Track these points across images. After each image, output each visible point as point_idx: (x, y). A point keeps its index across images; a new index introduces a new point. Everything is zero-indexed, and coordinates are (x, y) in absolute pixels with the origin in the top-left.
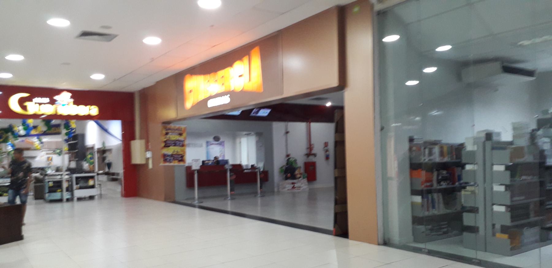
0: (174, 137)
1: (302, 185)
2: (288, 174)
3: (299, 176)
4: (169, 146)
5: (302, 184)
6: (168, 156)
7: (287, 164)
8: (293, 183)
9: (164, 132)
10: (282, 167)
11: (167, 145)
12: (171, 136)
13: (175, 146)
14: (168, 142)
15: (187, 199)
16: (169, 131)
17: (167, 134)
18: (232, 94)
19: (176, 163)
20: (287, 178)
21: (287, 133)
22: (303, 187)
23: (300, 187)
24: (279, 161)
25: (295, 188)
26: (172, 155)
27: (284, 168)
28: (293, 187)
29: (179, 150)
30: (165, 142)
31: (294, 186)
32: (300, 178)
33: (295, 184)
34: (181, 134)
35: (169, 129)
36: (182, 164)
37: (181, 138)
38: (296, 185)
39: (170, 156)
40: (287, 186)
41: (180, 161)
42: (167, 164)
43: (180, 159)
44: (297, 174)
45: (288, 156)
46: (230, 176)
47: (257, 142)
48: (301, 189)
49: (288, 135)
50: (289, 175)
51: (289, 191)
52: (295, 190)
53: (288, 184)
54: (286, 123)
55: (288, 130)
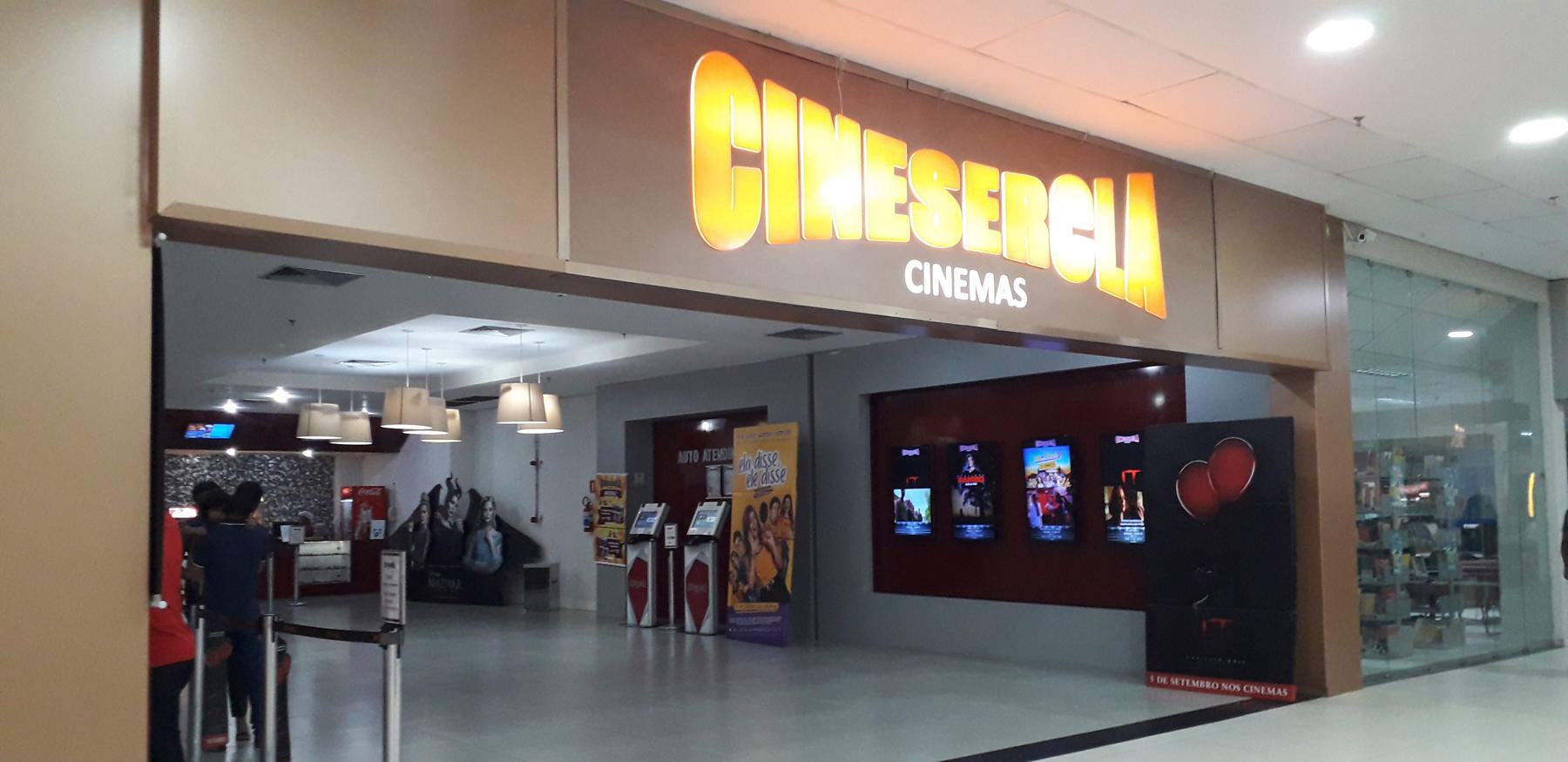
18: (1040, 279)
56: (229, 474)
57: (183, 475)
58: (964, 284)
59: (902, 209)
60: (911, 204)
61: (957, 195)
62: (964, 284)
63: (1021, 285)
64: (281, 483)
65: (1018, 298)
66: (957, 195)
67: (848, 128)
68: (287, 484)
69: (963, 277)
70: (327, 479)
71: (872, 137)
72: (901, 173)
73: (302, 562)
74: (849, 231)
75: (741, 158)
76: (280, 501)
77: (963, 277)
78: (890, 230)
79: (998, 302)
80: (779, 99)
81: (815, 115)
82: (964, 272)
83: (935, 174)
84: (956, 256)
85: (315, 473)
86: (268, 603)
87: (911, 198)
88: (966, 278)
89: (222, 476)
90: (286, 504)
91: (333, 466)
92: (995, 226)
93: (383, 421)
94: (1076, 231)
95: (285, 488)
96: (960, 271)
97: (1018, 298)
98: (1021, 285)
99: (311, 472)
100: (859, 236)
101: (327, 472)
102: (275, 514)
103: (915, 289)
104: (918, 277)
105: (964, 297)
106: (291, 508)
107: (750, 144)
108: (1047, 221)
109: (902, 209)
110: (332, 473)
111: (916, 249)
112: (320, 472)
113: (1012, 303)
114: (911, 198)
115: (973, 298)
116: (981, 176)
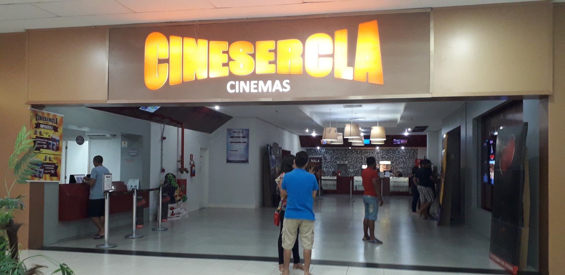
0: (47, 132)
1: (181, 211)
3: (178, 198)
7: (165, 182)
9: (34, 121)
12: (42, 130)
13: (48, 148)
15: (59, 241)
16: (41, 122)
17: (38, 126)
19: (47, 179)
21: (165, 138)
22: (182, 213)
23: (179, 213)
24: (155, 180)
25: (174, 215)
29: (52, 157)
32: (180, 200)
33: (174, 210)
34: (55, 129)
35: (41, 118)
36: (55, 180)
37: (56, 136)
38: (175, 211)
41: (52, 175)
42: (36, 180)
43: (53, 172)
45: (163, 170)
46: (138, 200)
47: (123, 151)
48: (181, 215)
49: (164, 141)
54: (163, 125)
55: (164, 136)
56: (383, 155)
57: (369, 155)
58: (256, 86)
59: (224, 65)
60: (231, 63)
61: (253, 56)
62: (256, 86)
63: (287, 83)
64: (400, 158)
65: (286, 88)
66: (253, 56)
67: (203, 43)
68: (402, 158)
69: (255, 84)
70: (415, 157)
71: (212, 43)
72: (227, 52)
73: (391, 184)
74: (202, 75)
75: (161, 61)
76: (400, 164)
77: (255, 84)
78: (218, 72)
79: (274, 91)
80: (176, 42)
81: (190, 43)
82: (256, 82)
83: (241, 50)
84: (254, 76)
85: (411, 154)
86: (56, 180)
87: (230, 59)
88: (257, 84)
89: (381, 156)
90: (402, 165)
91: (417, 152)
92: (274, 62)
93: (323, 137)
94: (320, 56)
95: (401, 159)
96: (253, 82)
97: (286, 88)
98: (287, 83)
99: (410, 154)
100: (206, 77)
101: (415, 154)
102: (398, 168)
103: (232, 91)
104: (233, 87)
105: (256, 91)
106: (403, 166)
107: (164, 56)
108: (303, 55)
109: (224, 65)
110: (417, 154)
111: (232, 77)
112: (413, 154)
113: (281, 90)
114: (230, 59)
115: (237, 91)
116: (265, 46)
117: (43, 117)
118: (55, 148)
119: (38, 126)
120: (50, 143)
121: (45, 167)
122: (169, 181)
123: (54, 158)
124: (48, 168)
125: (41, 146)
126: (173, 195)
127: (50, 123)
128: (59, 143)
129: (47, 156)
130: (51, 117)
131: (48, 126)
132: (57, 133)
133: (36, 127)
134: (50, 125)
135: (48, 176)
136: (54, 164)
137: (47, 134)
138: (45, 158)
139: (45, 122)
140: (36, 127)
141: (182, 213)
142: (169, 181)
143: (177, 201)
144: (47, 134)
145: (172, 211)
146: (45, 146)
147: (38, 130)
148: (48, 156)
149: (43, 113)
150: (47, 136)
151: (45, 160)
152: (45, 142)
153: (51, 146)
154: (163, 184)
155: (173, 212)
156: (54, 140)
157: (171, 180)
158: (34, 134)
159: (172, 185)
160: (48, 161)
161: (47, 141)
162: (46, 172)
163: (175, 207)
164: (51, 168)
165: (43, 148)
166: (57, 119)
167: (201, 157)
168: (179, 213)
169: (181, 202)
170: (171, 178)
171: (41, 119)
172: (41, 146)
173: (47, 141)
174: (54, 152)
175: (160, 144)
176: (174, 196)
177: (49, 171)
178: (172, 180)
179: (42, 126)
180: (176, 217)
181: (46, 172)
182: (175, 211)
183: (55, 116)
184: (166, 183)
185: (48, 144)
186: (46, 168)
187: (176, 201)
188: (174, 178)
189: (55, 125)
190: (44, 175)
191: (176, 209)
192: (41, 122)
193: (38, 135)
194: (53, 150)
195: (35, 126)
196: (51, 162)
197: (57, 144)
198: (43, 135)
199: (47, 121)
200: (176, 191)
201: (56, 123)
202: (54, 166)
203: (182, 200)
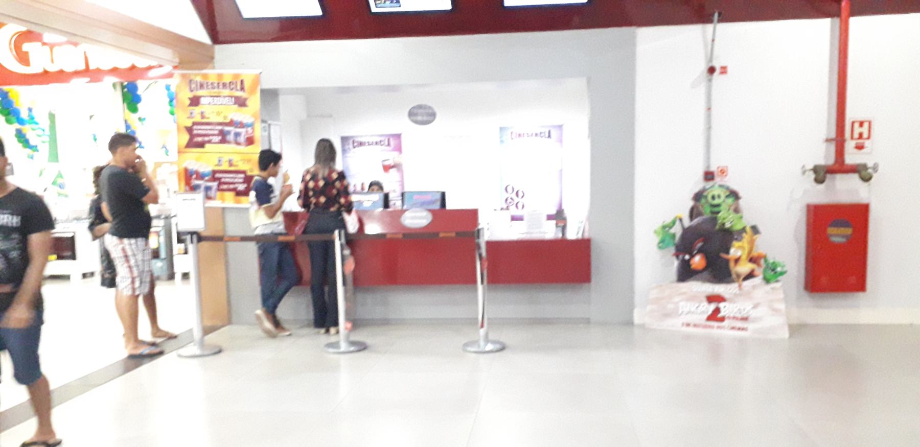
1: (753, 314)
2: (692, 256)
3: (744, 268)
4: (201, 145)
5: (755, 307)
6: (200, 176)
7: (693, 213)
8: (711, 299)
9: (185, 96)
10: (666, 228)
11: (195, 142)
13: (223, 141)
14: (197, 130)
17: (195, 101)
20: (686, 273)
23: (745, 319)
25: (722, 319)
26: (214, 176)
27: (677, 230)
28: (715, 316)
29: (236, 158)
30: (189, 130)
31: (717, 310)
32: (750, 276)
33: (722, 305)
34: (241, 103)
39: (207, 178)
40: (685, 306)
44: (737, 260)
48: (750, 326)
50: (698, 261)
51: (691, 330)
52: (717, 331)
53: (693, 298)
117: (207, 83)
118: (242, 139)
119: (195, 101)
120: (229, 132)
121: (219, 179)
122: (707, 211)
123: (243, 160)
124: (227, 180)
125: (206, 139)
126: (724, 256)
127: (226, 92)
128: (253, 129)
129: (222, 157)
130: (227, 80)
131: (221, 99)
132: (244, 109)
133: (191, 105)
134: (225, 97)
135: (230, 195)
136: (244, 172)
137: (218, 114)
138: (219, 161)
139: (215, 91)
140: (191, 105)
141: (756, 320)
142: (707, 211)
143: (738, 276)
144: (218, 114)
145: (712, 307)
146: (219, 138)
147: (197, 110)
148: (226, 158)
149: (205, 76)
150: (221, 120)
151: (219, 165)
152: (217, 130)
153: (231, 137)
154: (681, 220)
155: (717, 310)
156: (241, 125)
157: (718, 205)
158: (188, 118)
159: (724, 224)
160: (225, 167)
161: (220, 128)
162: (225, 187)
163: (726, 296)
164: (236, 180)
165: (209, 142)
166: (242, 82)
167: (536, 135)
168: (745, 319)
169: (757, 280)
170: (716, 202)
171: (202, 86)
172: (206, 139)
173: (220, 128)
174: (242, 149)
175: (702, 90)
176: (727, 261)
177: (232, 186)
178: (723, 208)
179: (203, 100)
180: (733, 328)
181: (225, 187)
182: (726, 309)
183: (236, 76)
184: (696, 217)
185: (223, 134)
186: (223, 180)
187: (734, 276)
188: (730, 201)
189: (239, 94)
190: (219, 193)
191: (732, 301)
192: (200, 93)
193: (198, 119)
194: (238, 144)
195: (188, 102)
196: (232, 169)
197: (247, 132)
198: (208, 118)
199: (216, 90)
200: (736, 244)
201: (242, 89)
202: (242, 176)
203: (761, 277)
